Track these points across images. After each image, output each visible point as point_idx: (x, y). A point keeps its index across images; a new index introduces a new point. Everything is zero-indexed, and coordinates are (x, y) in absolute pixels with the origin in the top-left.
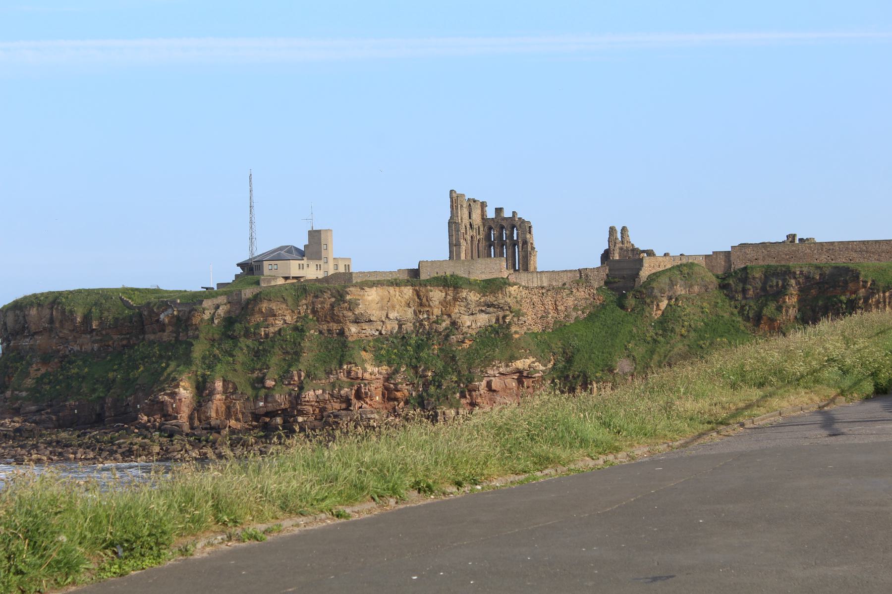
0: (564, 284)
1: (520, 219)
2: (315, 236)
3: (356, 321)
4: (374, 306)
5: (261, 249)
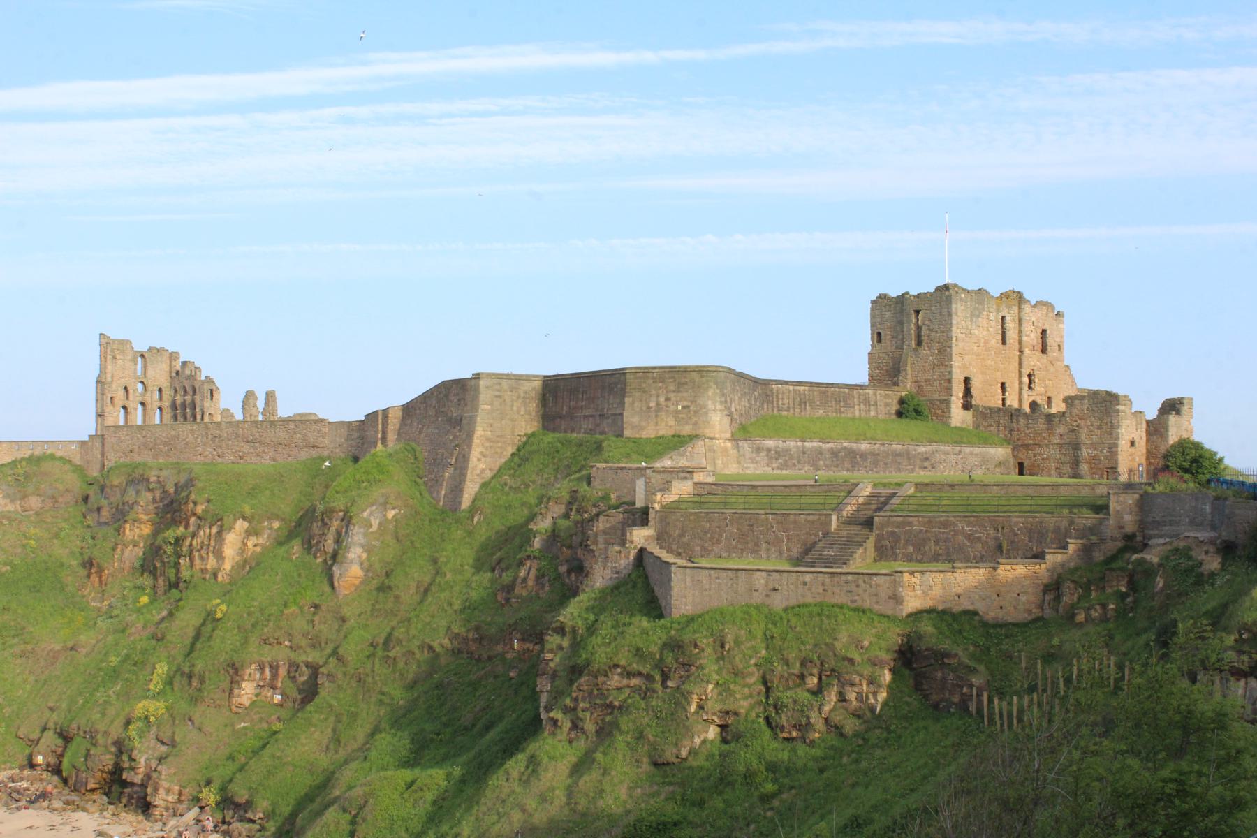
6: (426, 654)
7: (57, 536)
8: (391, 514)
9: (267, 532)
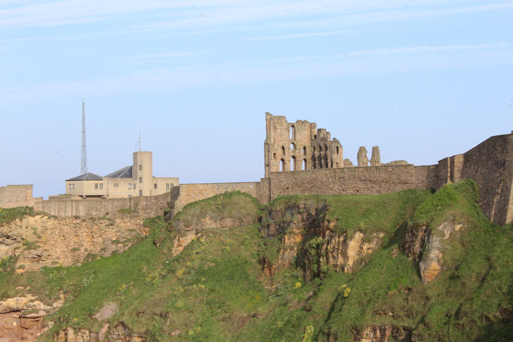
0: (107, 214)
1: (334, 139)
6: (484, 323)
7: (243, 243)
8: (458, 227)
9: (375, 241)
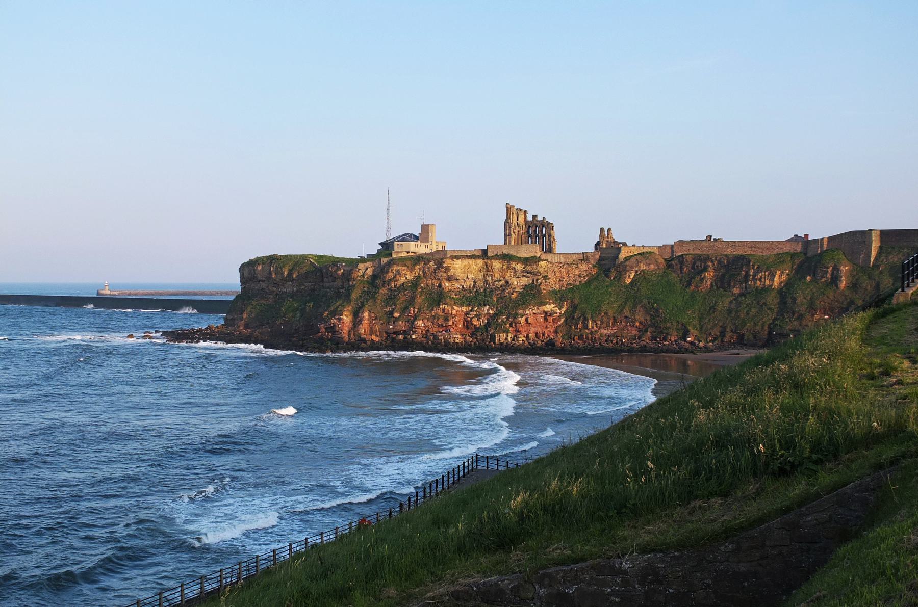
2: (425, 228)
3: (449, 279)
4: (459, 270)
5: (393, 235)
